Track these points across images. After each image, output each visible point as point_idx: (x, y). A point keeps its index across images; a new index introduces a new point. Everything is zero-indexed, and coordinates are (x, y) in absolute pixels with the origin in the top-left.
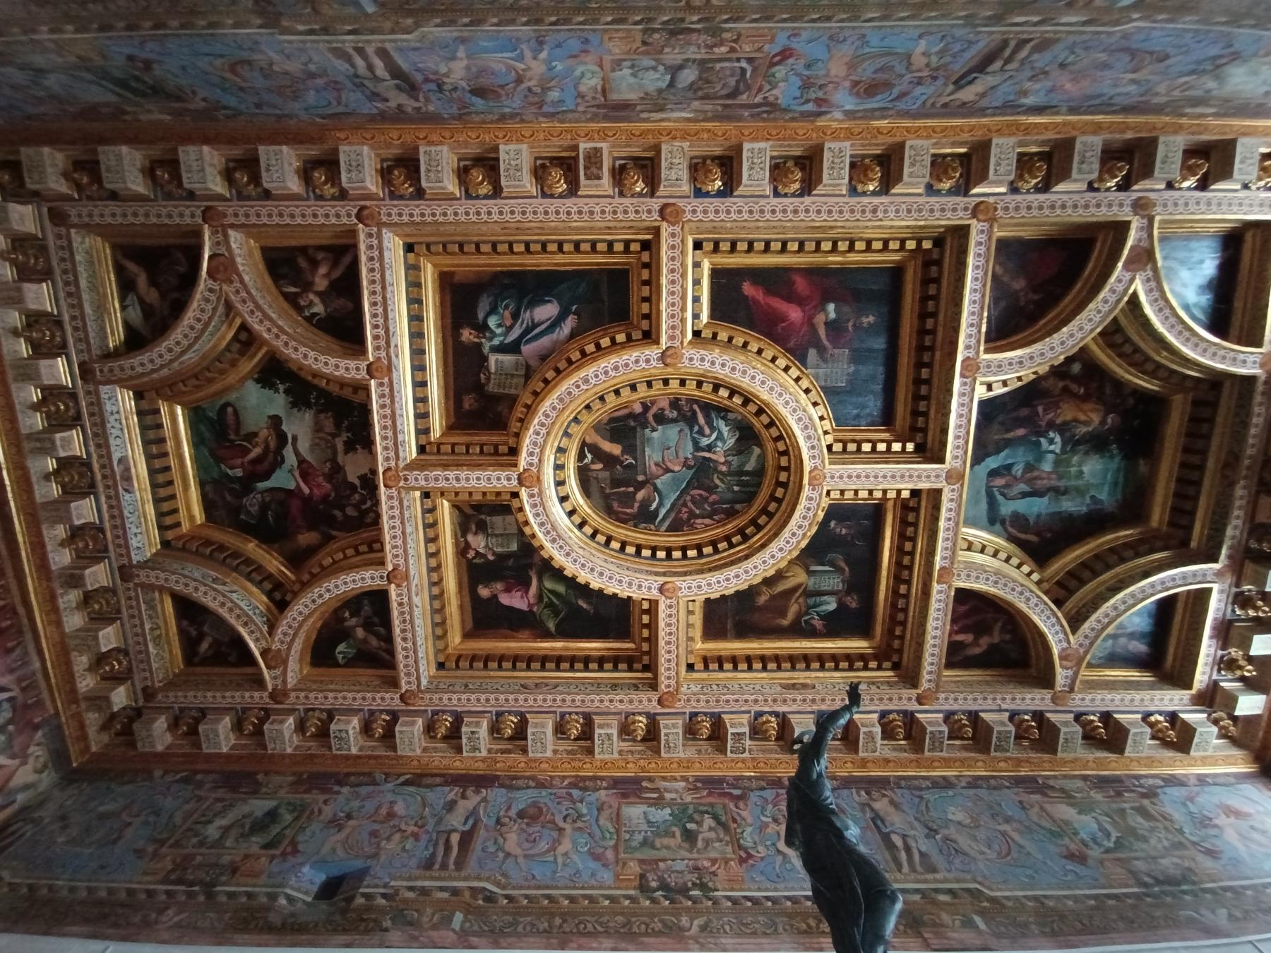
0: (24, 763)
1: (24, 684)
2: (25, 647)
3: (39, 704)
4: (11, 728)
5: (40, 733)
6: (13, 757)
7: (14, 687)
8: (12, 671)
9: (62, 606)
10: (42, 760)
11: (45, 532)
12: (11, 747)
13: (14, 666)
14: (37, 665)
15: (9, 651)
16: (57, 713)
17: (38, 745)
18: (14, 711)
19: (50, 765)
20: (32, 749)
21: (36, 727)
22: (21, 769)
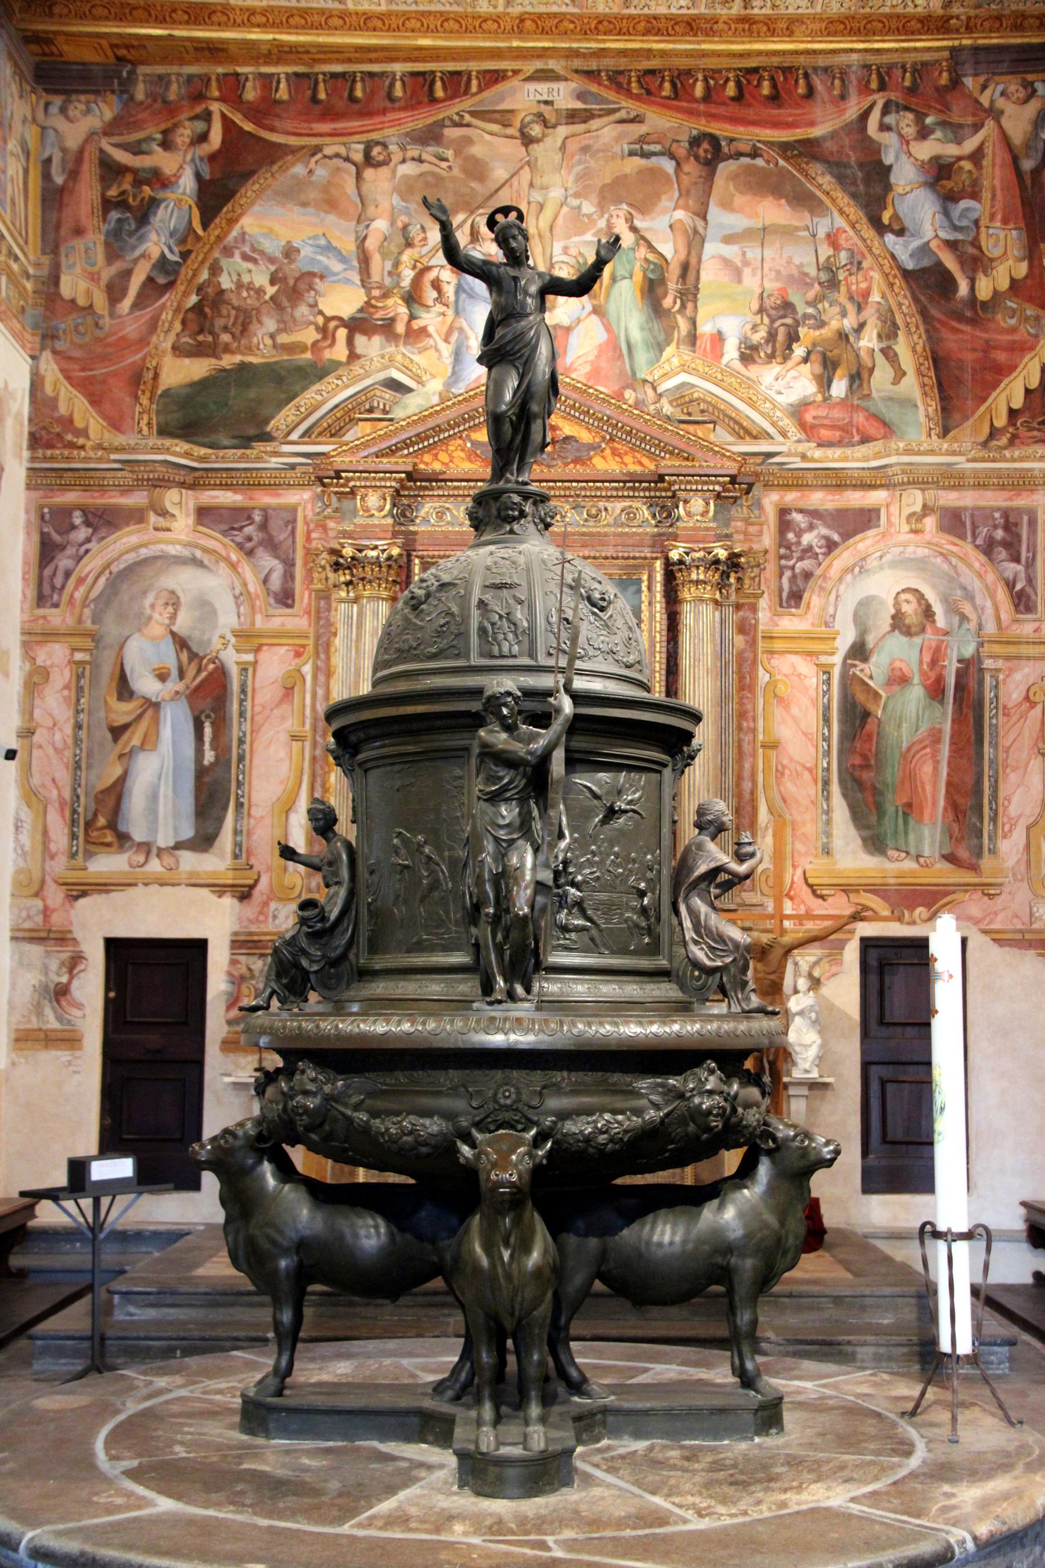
0: (996, 114)
1: (874, 85)
2: (815, 69)
3: (921, 70)
4: (929, 120)
5: (969, 82)
6: (977, 127)
7: (871, 98)
8: (843, 97)
9: (768, 11)
10: (1012, 88)
11: (632, 11)
12: (961, 126)
13: (836, 92)
14: (855, 56)
15: (811, 92)
16: (952, 49)
17: (984, 87)
18: (907, 108)
19: (1030, 77)
20: (985, 100)
21: (956, 83)
22: (1004, 122)
